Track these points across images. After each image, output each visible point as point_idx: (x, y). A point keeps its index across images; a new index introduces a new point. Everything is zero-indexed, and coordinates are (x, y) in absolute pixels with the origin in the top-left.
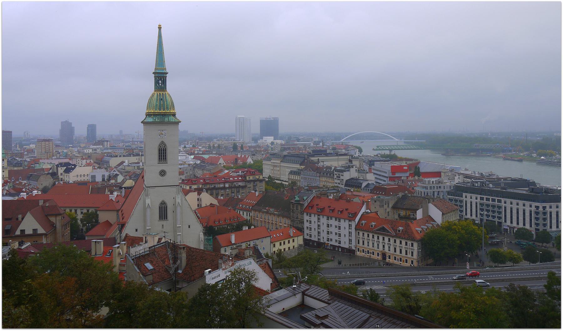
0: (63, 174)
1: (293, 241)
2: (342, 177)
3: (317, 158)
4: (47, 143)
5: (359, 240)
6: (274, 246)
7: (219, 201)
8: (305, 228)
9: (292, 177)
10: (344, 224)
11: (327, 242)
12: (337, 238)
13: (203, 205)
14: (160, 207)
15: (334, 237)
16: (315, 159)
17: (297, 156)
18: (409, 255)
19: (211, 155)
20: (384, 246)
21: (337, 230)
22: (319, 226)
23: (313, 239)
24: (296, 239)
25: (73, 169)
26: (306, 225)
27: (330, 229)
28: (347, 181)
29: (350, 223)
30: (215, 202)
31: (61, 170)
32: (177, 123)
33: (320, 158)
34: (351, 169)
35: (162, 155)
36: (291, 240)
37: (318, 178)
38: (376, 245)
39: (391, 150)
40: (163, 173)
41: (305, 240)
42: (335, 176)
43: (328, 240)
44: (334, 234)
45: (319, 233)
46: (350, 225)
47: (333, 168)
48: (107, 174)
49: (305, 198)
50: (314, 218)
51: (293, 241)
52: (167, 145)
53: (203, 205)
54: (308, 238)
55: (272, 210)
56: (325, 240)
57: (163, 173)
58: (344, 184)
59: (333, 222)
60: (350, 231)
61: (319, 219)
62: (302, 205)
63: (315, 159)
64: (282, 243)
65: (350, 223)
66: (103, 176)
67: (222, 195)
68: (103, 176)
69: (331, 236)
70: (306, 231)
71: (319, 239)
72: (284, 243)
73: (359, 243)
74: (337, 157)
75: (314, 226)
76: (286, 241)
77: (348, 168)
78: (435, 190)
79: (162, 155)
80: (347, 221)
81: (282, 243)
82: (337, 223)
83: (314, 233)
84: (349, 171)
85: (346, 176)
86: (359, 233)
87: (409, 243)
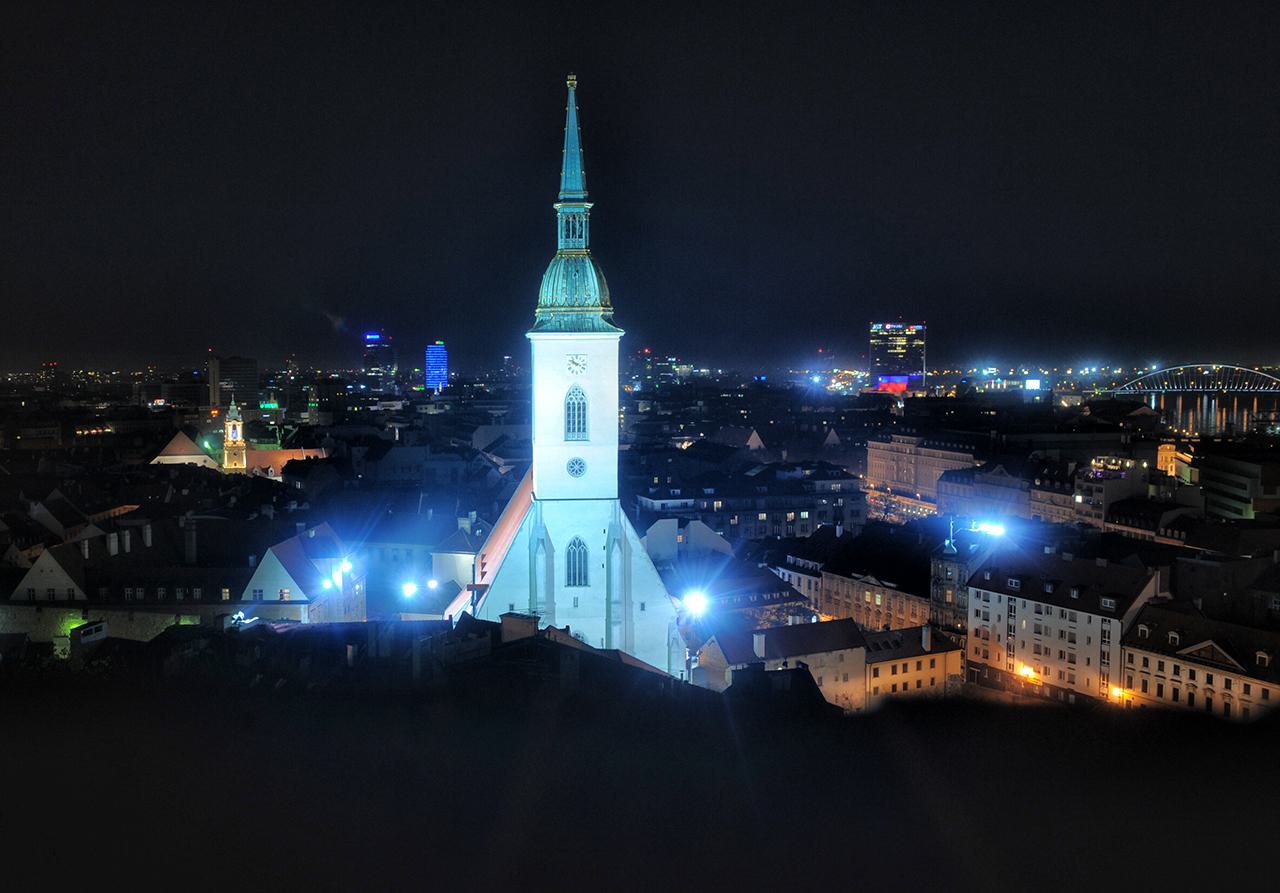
1: (933, 663)
14: (569, 553)
24: (939, 657)
26: (973, 623)
29: (1106, 627)
40: (576, 467)
41: (969, 665)
51: (933, 663)
54: (979, 659)
60: (1105, 648)
61: (1011, 609)
65: (1106, 627)
70: (972, 642)
80: (1097, 619)
82: (1065, 625)
86: (1131, 656)
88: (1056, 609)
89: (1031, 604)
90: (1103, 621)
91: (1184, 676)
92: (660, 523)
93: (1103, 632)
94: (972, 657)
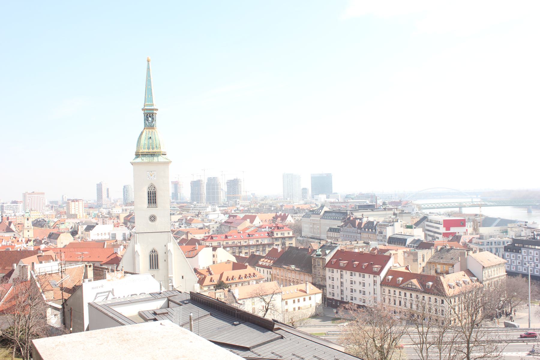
0: (84, 232)
1: (310, 299)
2: (384, 234)
3: (361, 214)
4: (77, 203)
5: (384, 299)
6: (287, 303)
7: (237, 258)
8: (328, 286)
9: (331, 234)
10: (369, 279)
11: (350, 301)
12: (361, 296)
13: (219, 262)
14: (150, 256)
15: (357, 295)
16: (358, 215)
17: (339, 212)
18: (439, 314)
19: (247, 214)
20: (411, 304)
21: (361, 288)
22: (342, 283)
23: (336, 298)
25: (93, 227)
26: (328, 282)
27: (354, 287)
28: (390, 238)
29: (375, 279)
30: (234, 260)
31: (82, 229)
32: (168, 163)
33: (365, 213)
34: (396, 224)
35: (152, 198)
36: (307, 298)
37: (359, 235)
38: (403, 303)
39: (460, 207)
41: (324, 298)
42: (377, 233)
43: (352, 300)
44: (358, 291)
45: (342, 291)
46: (375, 282)
47: (375, 223)
48: (127, 232)
49: (327, 252)
50: (337, 274)
51: (310, 299)
52: (156, 187)
53: (219, 262)
55: (293, 267)
56: (349, 299)
57: (153, 218)
58: (387, 240)
59: (357, 277)
61: (341, 275)
62: (324, 260)
63: (358, 215)
64: (296, 301)
65: (375, 279)
66: (124, 234)
67: (246, 253)
68: (124, 234)
69: (354, 295)
70: (329, 290)
71: (342, 298)
72: (299, 301)
73: (384, 302)
74: (384, 212)
75: (337, 283)
76: (301, 299)
77: (391, 223)
78: (493, 246)
79: (152, 198)
80: (372, 276)
81: (296, 301)
82: (361, 279)
83: (337, 291)
84: (392, 225)
85: (389, 232)
87: (439, 299)
88: (357, 274)
89: (349, 273)
90: (374, 276)
91: (403, 294)
92: (205, 249)
93: (374, 281)
94: (329, 296)
